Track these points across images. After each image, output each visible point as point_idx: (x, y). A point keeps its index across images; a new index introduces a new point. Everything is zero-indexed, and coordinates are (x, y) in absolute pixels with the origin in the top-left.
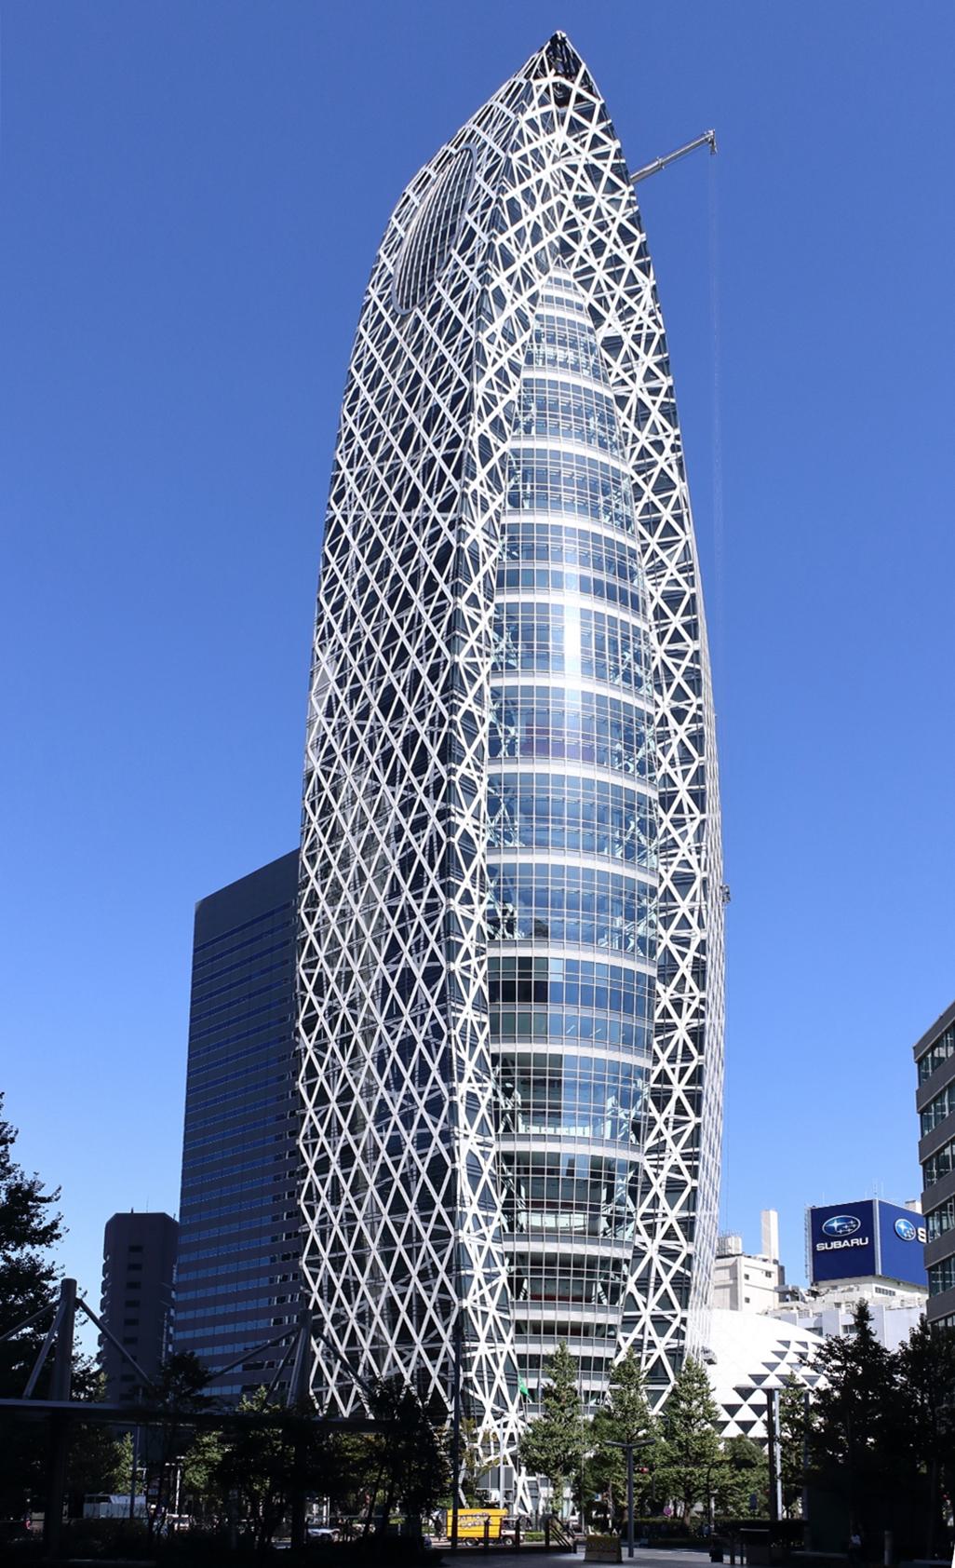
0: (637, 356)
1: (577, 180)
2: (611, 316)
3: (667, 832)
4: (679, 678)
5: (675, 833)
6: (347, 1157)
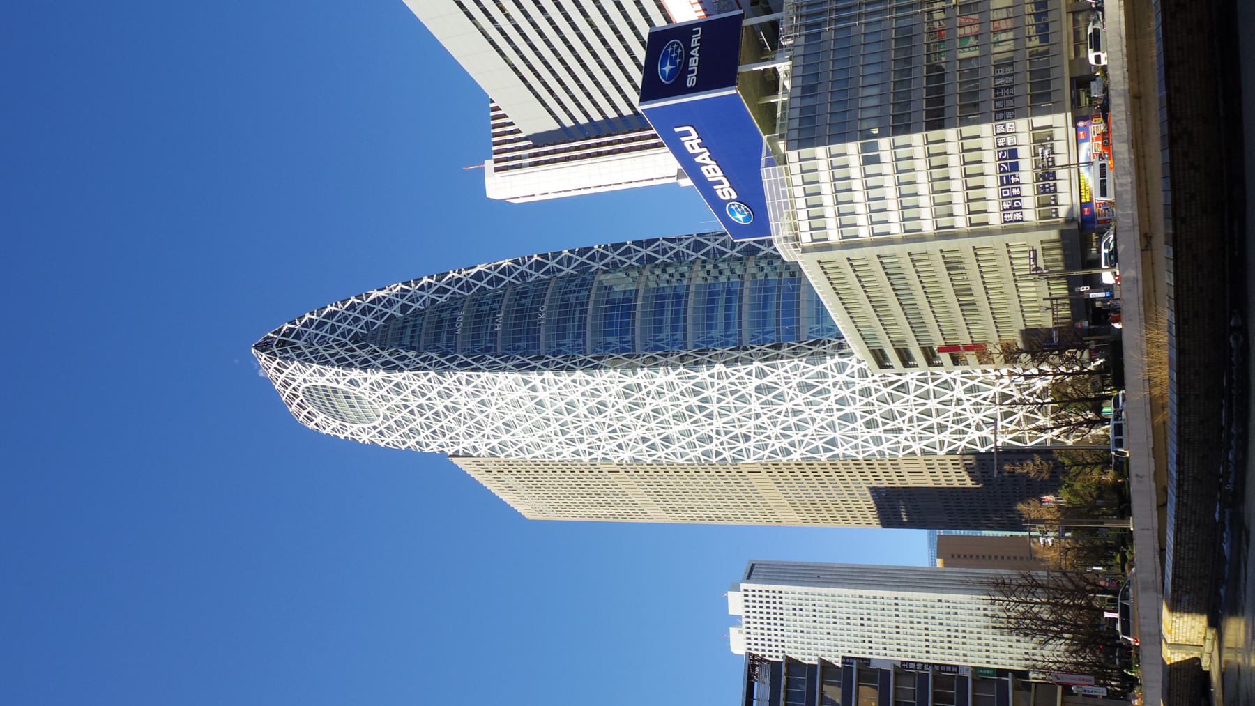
1: (321, 333)
2: (390, 311)
3: (670, 258)
4: (584, 259)
5: (671, 253)
6: (870, 424)
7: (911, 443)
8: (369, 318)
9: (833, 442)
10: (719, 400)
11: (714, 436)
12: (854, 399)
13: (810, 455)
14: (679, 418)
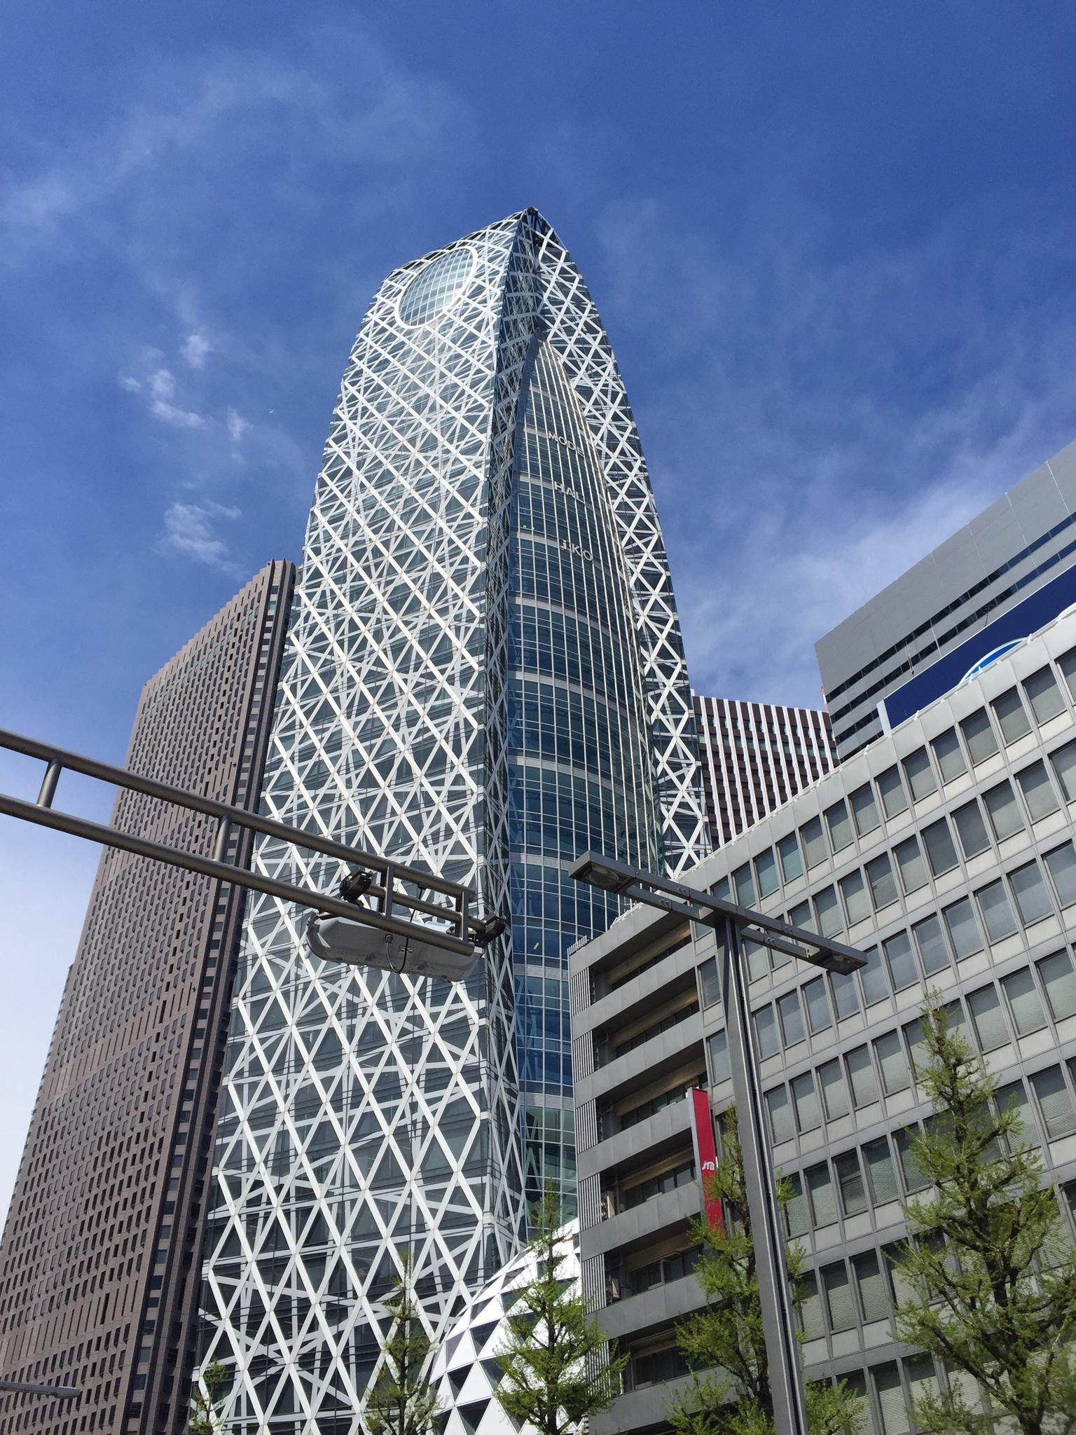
0: (605, 404)
4: (662, 640)
5: (673, 776)
6: (306, 1104)
7: (246, 1194)
8: (571, 346)
9: (275, 1021)
10: (400, 797)
11: (322, 792)
12: (374, 1061)
13: (251, 973)
14: (370, 731)
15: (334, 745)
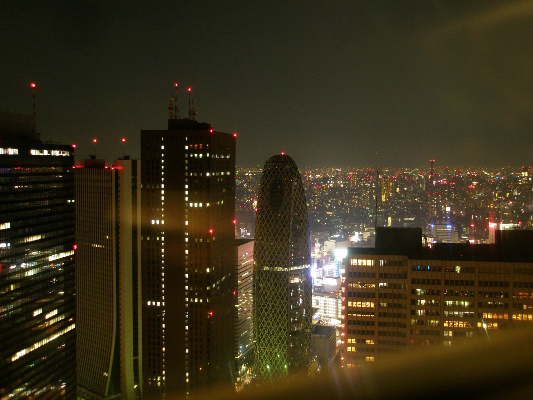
8: (300, 208)
9: (264, 339)
14: (273, 306)
15: (268, 306)
